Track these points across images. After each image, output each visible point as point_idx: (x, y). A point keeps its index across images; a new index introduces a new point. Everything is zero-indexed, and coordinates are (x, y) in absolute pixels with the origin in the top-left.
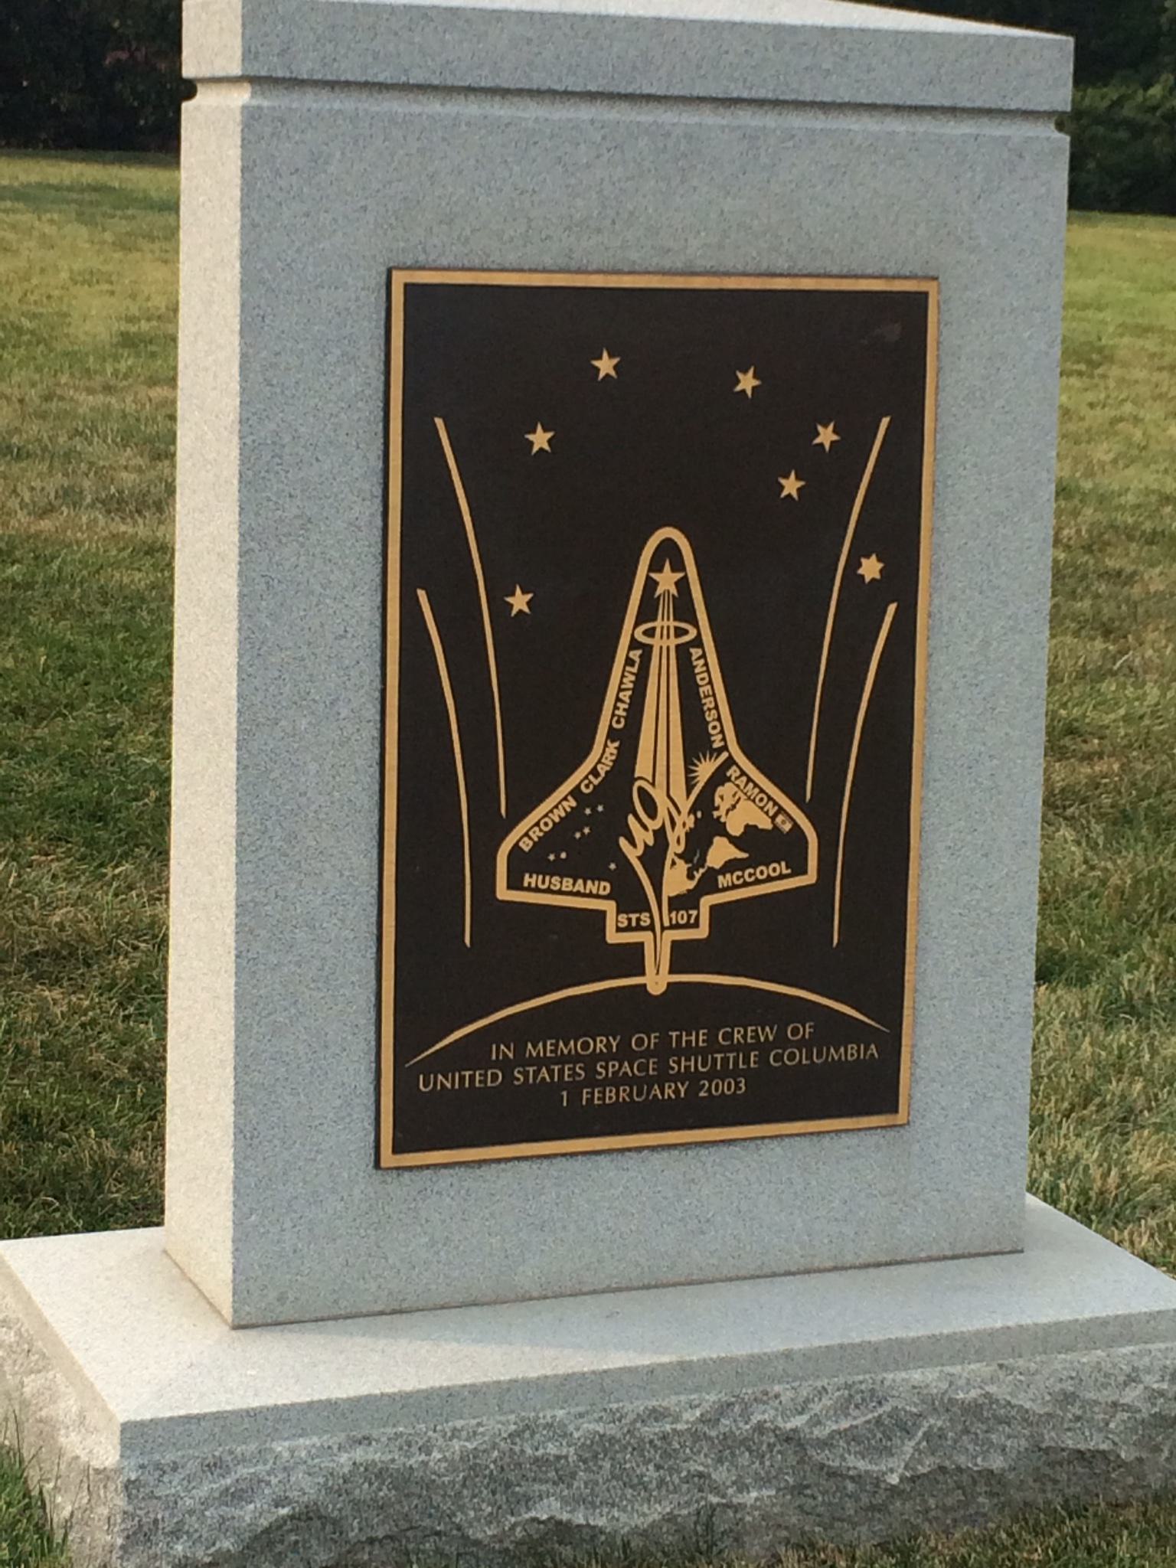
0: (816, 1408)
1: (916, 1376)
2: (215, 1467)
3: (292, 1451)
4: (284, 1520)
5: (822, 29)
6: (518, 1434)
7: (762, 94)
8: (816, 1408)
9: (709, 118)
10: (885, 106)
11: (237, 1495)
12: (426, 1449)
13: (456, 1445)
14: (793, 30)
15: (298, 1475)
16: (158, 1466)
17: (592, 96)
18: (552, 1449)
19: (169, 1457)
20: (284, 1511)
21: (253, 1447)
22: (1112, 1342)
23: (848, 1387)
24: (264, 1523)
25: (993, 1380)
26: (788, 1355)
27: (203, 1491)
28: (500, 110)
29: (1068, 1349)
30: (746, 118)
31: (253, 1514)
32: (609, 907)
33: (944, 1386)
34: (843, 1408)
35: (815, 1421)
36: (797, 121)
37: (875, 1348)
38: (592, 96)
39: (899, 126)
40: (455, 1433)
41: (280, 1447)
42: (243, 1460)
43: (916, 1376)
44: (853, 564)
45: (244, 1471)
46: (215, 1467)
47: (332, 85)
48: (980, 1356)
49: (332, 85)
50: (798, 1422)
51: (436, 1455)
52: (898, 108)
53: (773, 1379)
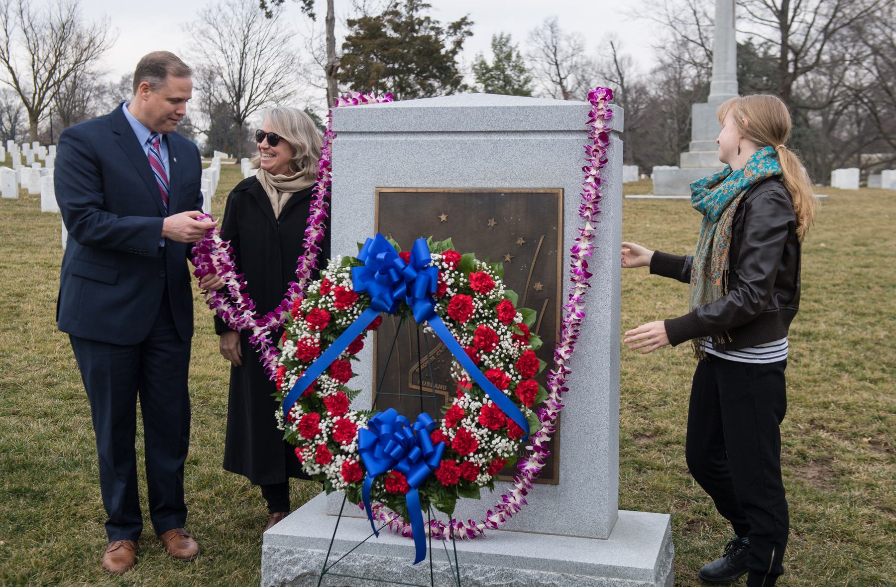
0: (488, 575)
1: (528, 572)
2: (290, 552)
3: (313, 553)
4: (307, 574)
5: (519, 107)
6: (385, 562)
7: (498, 129)
8: (488, 575)
9: (482, 138)
10: (543, 131)
11: (295, 563)
12: (354, 561)
13: (364, 561)
14: (509, 108)
15: (312, 560)
16: (274, 549)
17: (442, 132)
18: (395, 570)
19: (277, 547)
20: (305, 571)
21: (302, 549)
22: (608, 575)
23: (502, 570)
24: (300, 573)
25: (559, 579)
26: (480, 554)
27: (283, 560)
28: (411, 138)
29: (591, 575)
30: (495, 137)
31: (297, 570)
32: (446, 394)
33: (537, 577)
34: (500, 577)
35: (487, 580)
36: (512, 137)
37: (513, 558)
38: (442, 132)
39: (549, 137)
40: (365, 557)
41: (310, 551)
42: (298, 553)
43: (528, 572)
44: (532, 284)
45: (297, 556)
46: (290, 552)
47: (361, 133)
48: (554, 570)
49: (361, 133)
50: (480, 578)
51: (357, 563)
52: (549, 132)
53: (475, 562)
